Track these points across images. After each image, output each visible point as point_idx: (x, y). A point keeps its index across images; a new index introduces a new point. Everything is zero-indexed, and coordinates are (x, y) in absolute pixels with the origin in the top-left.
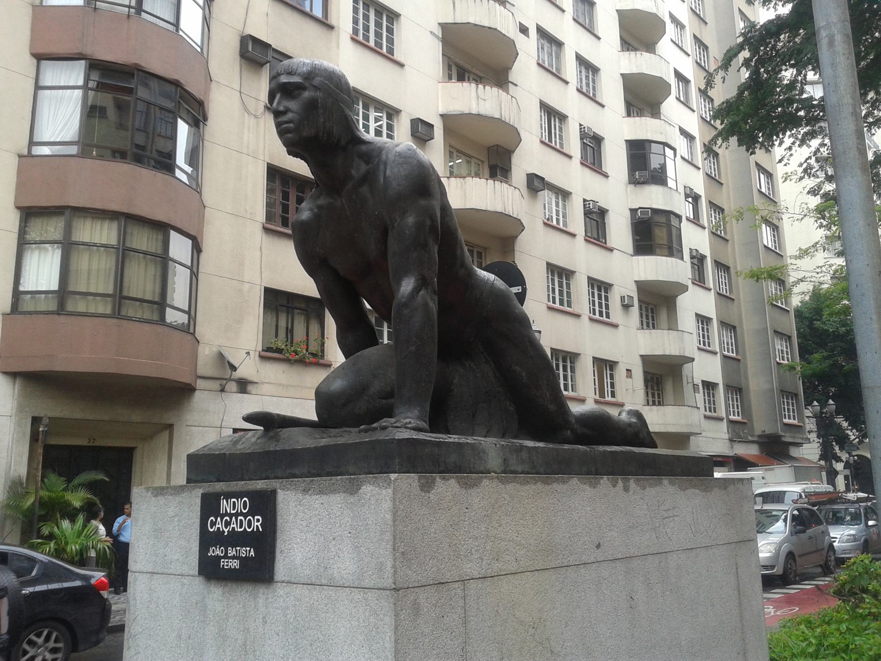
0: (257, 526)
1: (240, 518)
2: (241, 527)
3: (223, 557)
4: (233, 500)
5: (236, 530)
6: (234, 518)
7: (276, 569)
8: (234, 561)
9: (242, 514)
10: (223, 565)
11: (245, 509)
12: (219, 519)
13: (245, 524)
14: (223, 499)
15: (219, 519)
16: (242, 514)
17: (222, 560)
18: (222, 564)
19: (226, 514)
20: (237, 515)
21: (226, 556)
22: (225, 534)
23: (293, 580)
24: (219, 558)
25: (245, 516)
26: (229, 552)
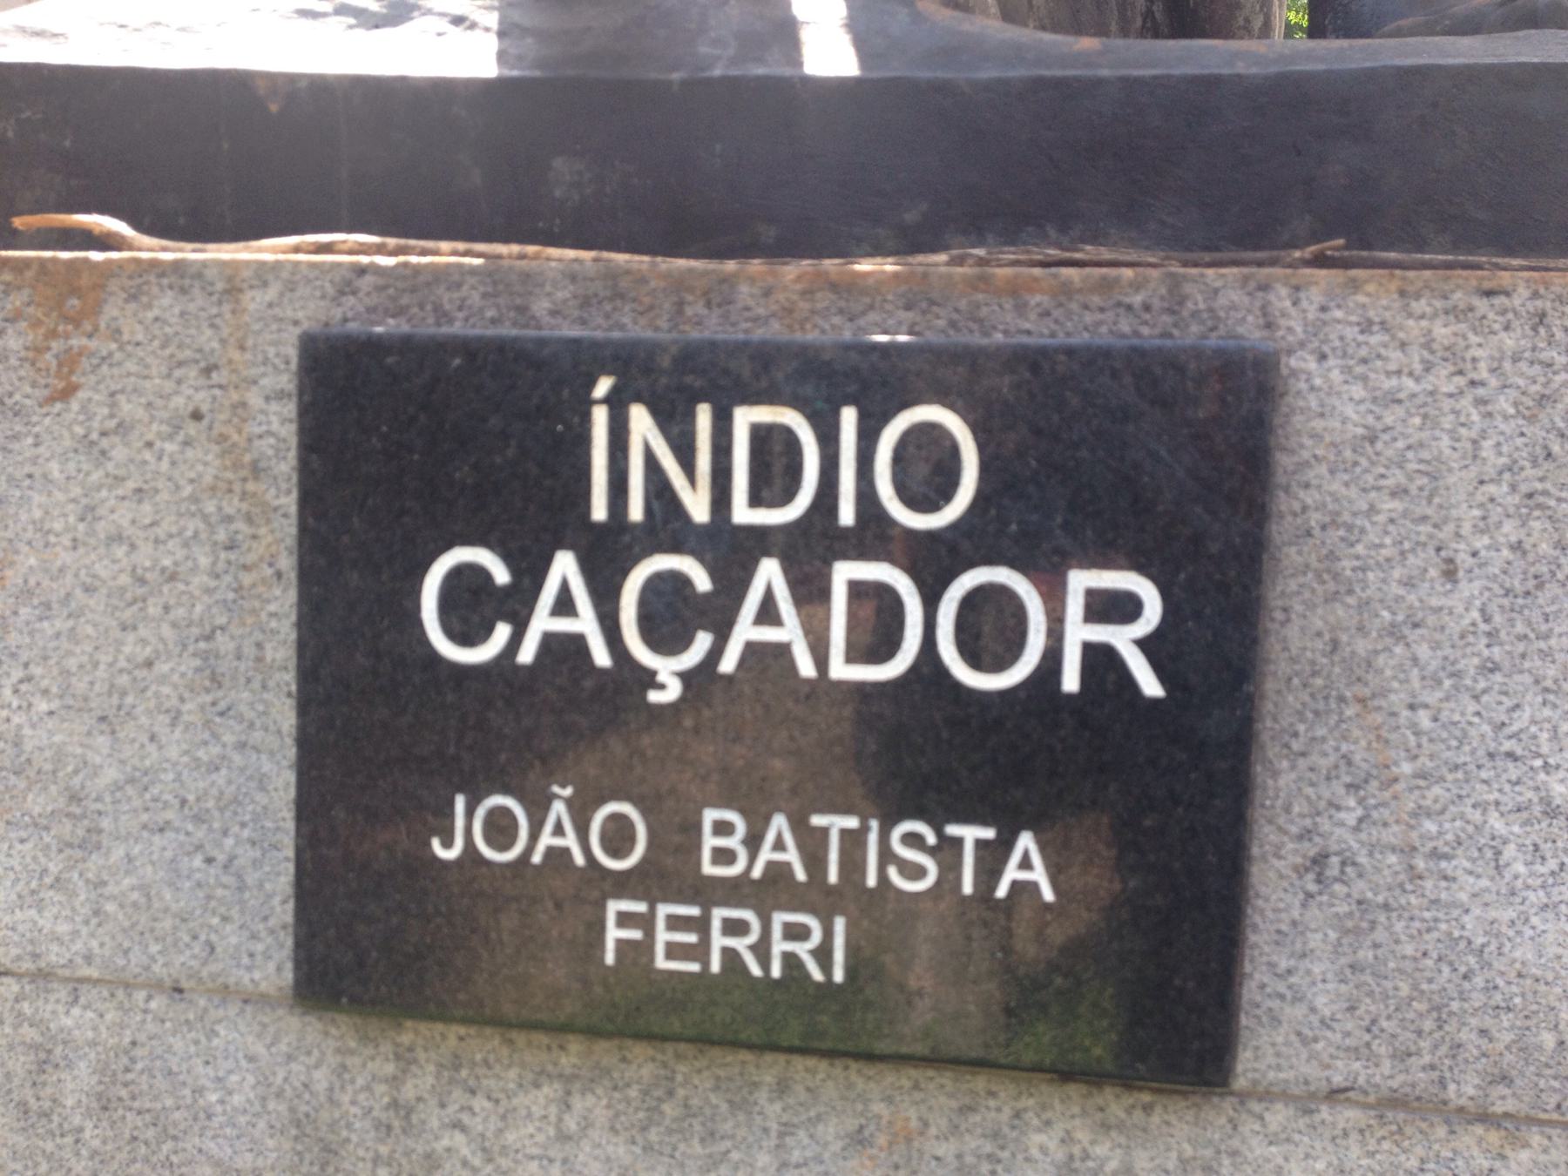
0: (1100, 659)
1: (845, 573)
3: (623, 884)
4: (745, 418)
5: (806, 667)
6: (769, 572)
7: (1249, 992)
8: (780, 919)
12: (565, 566)
14: (617, 405)
15: (565, 566)
17: (614, 907)
18: (614, 934)
22: (654, 697)
23: (1465, 1089)
26: (710, 842)
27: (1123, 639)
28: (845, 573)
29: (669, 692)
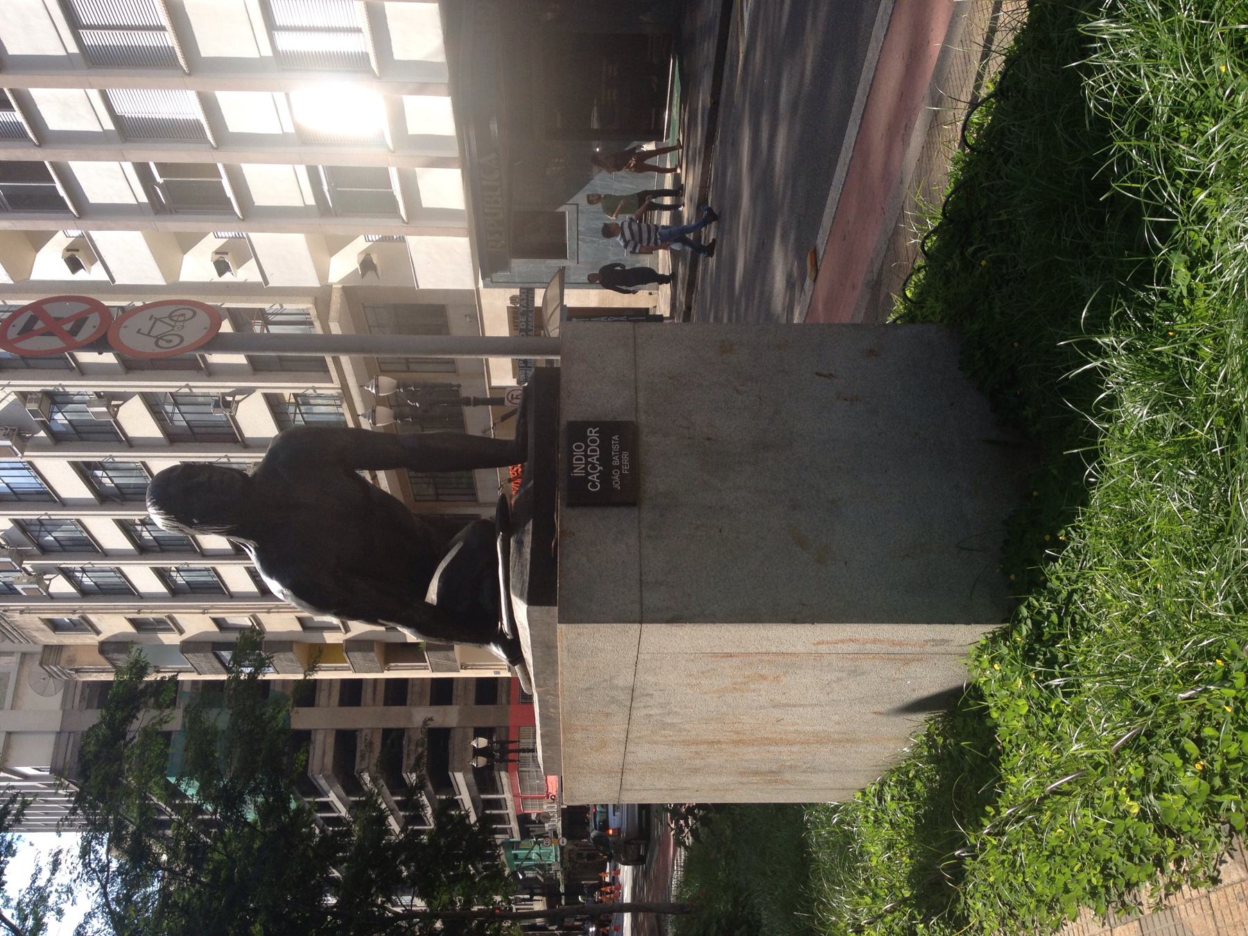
0: (595, 433)
2: (596, 451)
3: (621, 471)
6: (589, 460)
9: (585, 451)
10: (627, 470)
11: (581, 447)
12: (590, 478)
13: (593, 446)
15: (590, 478)
16: (585, 451)
19: (585, 469)
20: (587, 456)
21: (619, 467)
24: (622, 476)
27: (594, 431)
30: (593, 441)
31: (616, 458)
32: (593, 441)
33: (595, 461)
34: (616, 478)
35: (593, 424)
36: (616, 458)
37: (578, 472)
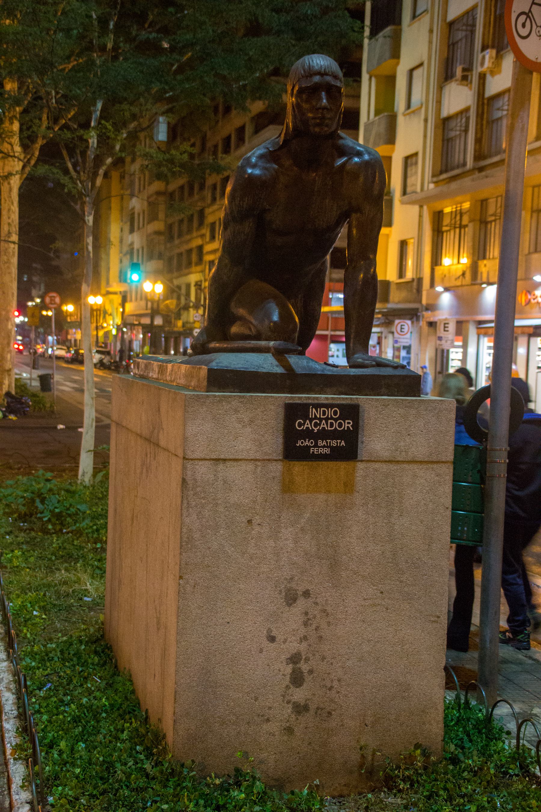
0: (348, 427)
1: (329, 421)
6: (324, 421)
9: (332, 418)
10: (313, 452)
12: (308, 421)
13: (336, 425)
15: (308, 421)
16: (332, 418)
19: (316, 418)
21: (316, 446)
24: (308, 447)
25: (336, 420)
27: (349, 425)
28: (329, 421)
29: (316, 431)
30: (340, 425)
31: (324, 443)
32: (340, 425)
33: (322, 426)
34: (307, 443)
35: (356, 426)
36: (324, 443)
37: (313, 412)
